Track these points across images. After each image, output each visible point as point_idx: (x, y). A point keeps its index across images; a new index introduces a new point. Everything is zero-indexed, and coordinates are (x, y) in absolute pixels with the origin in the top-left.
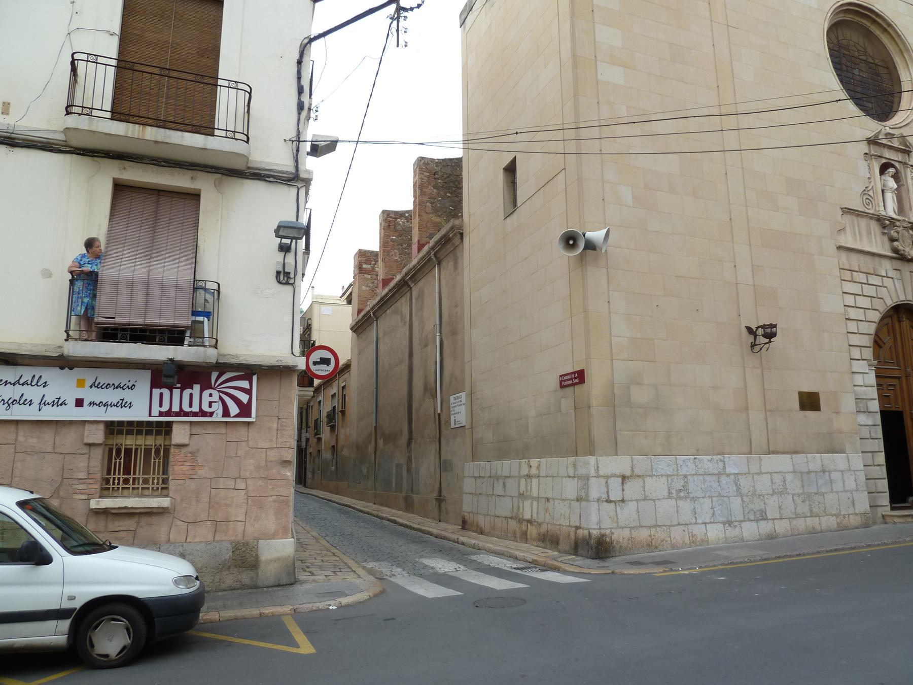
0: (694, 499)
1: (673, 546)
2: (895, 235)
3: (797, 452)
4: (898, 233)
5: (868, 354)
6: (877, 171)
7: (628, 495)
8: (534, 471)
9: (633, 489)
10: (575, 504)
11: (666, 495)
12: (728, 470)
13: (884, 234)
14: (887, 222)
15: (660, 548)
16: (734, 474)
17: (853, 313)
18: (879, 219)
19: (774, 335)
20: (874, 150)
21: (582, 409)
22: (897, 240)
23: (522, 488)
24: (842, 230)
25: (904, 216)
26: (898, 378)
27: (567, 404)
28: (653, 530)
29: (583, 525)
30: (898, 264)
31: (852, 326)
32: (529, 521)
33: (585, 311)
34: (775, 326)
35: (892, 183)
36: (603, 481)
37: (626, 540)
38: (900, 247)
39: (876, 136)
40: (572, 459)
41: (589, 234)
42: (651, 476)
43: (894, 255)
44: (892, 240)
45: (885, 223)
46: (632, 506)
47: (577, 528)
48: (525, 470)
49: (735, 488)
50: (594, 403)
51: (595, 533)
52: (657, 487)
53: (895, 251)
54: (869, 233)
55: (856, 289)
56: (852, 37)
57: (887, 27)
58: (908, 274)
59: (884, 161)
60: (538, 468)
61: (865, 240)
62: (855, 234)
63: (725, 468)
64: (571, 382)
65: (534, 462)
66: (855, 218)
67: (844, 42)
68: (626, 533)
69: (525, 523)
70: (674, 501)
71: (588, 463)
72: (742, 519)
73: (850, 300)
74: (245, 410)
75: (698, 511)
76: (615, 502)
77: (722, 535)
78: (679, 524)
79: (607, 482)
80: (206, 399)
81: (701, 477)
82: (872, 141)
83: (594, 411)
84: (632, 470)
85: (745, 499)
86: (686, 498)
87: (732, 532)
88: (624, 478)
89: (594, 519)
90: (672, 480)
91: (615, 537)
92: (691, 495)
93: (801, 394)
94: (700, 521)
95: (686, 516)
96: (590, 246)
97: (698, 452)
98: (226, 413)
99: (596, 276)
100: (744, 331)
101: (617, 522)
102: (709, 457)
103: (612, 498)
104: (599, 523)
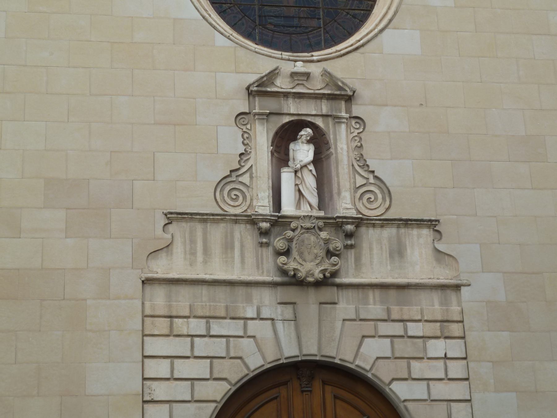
18: (252, 221)
30: (292, 293)
45: (272, 227)
53: (284, 272)
54: (228, 246)
55: (180, 347)
59: (286, 119)
62: (193, 253)
73: (160, 369)
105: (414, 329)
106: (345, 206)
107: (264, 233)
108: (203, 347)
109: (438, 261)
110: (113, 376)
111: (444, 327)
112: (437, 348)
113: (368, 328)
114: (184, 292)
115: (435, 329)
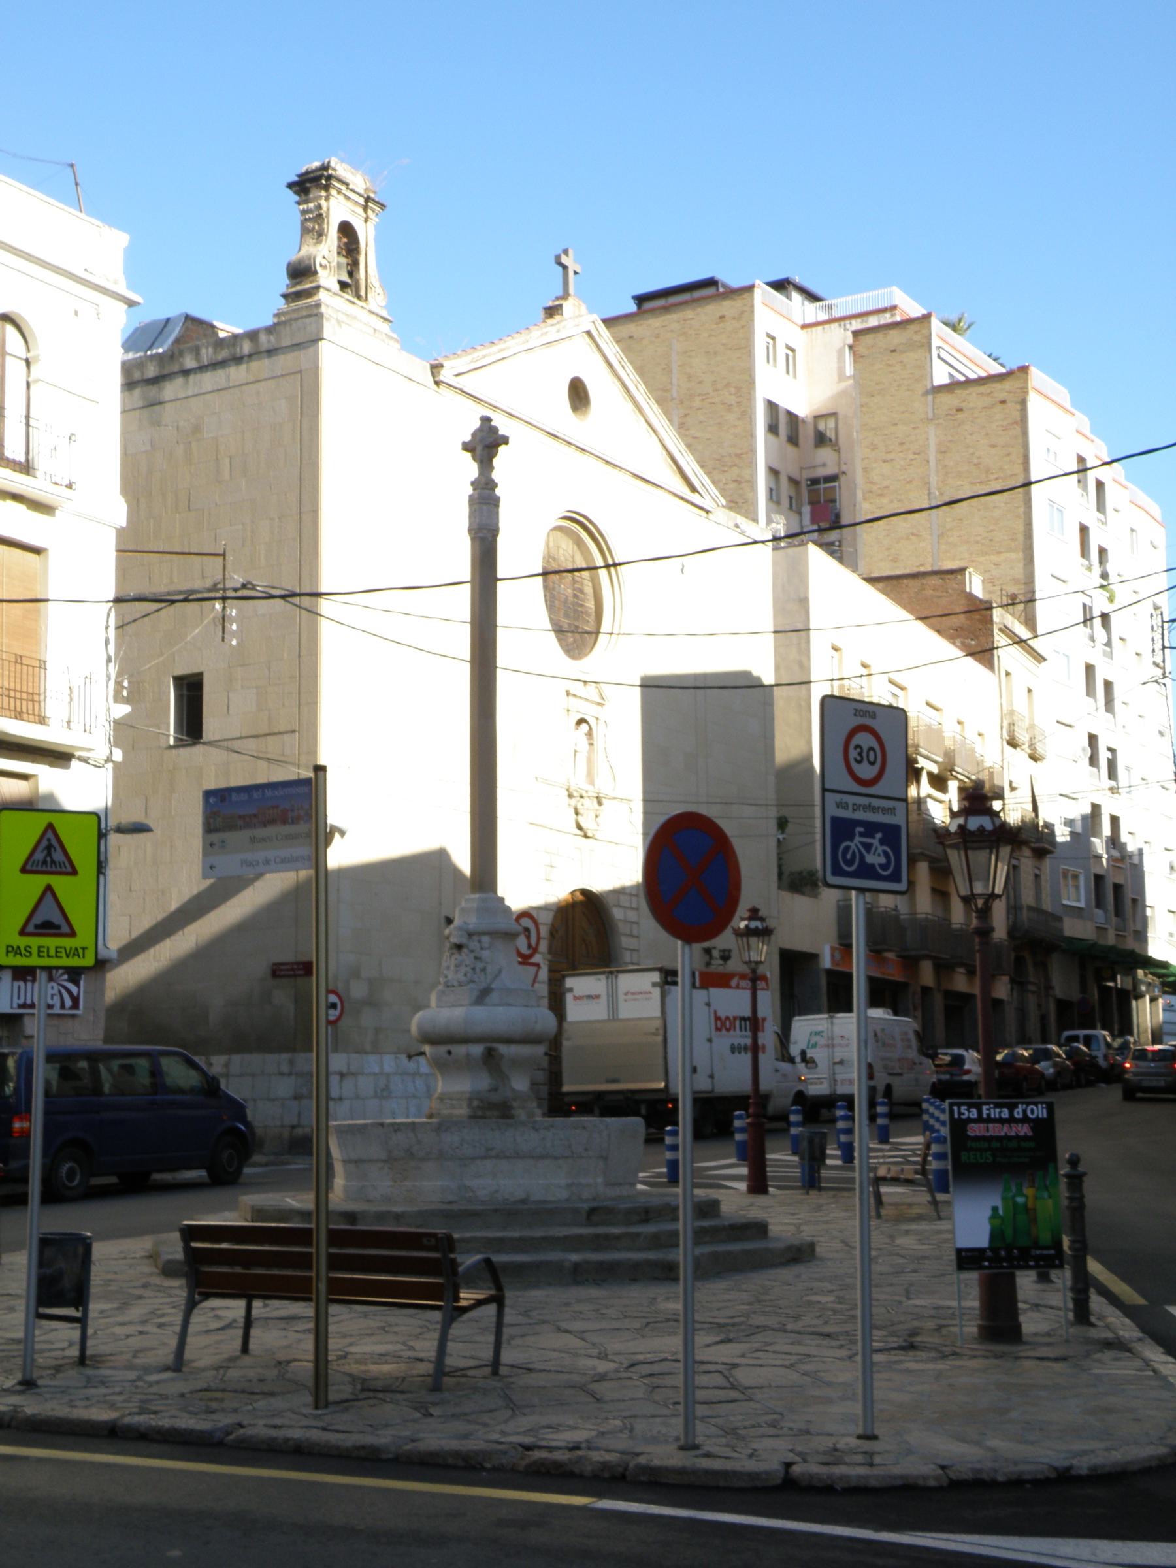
9: (348, 1084)
21: (303, 1002)
40: (285, 1056)
46: (347, 1103)
47: (293, 1127)
60: (227, 1065)
74: (75, 1001)
80: (50, 992)
98: (63, 1006)
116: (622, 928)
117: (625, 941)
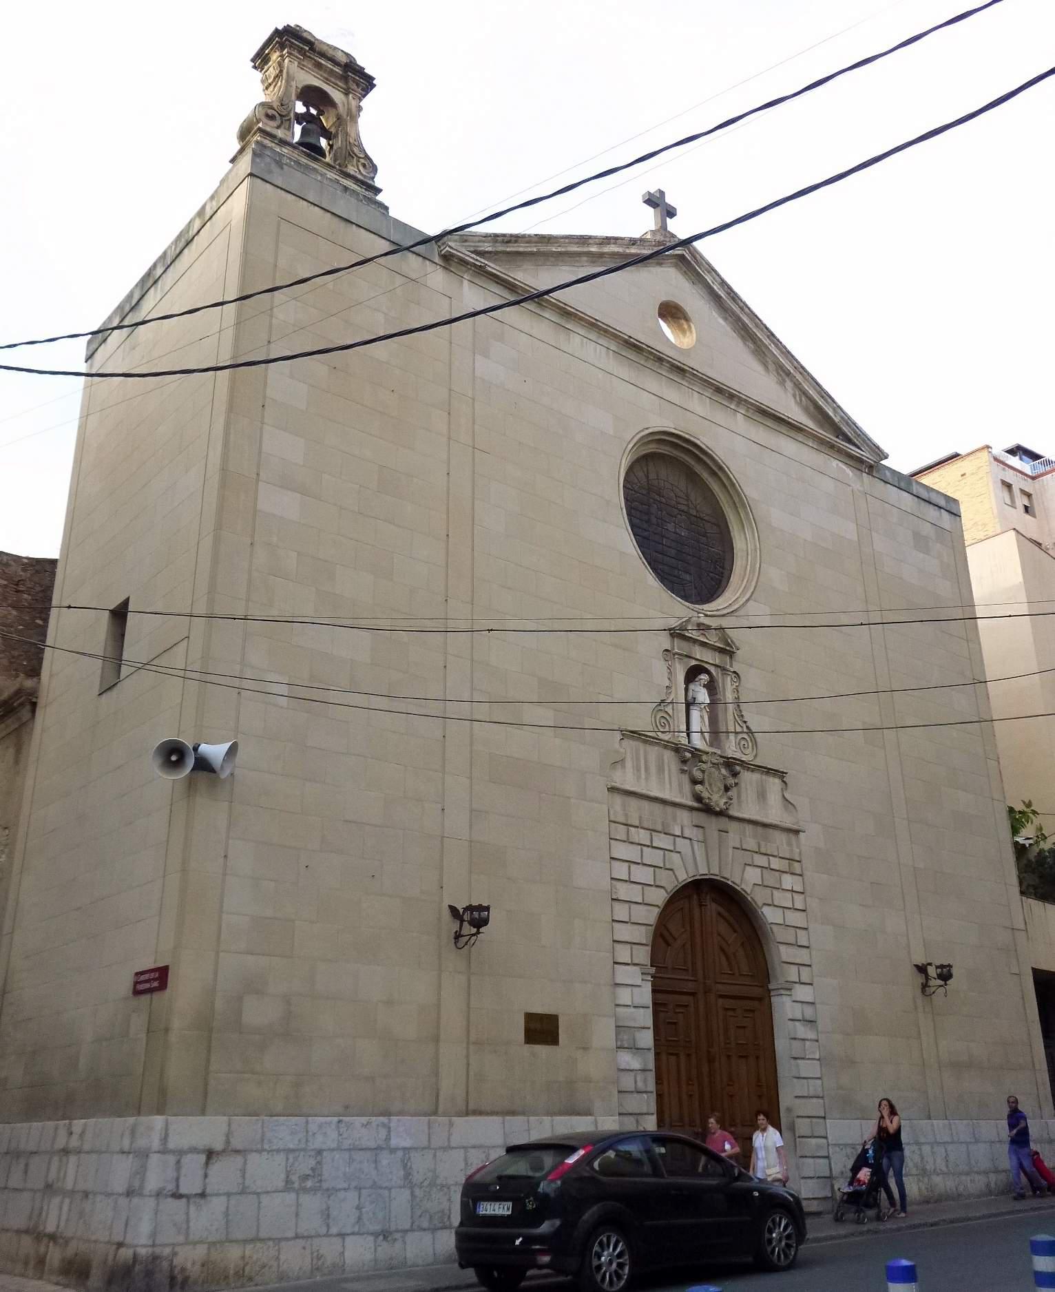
0: (330, 1192)
1: (282, 1277)
2: (698, 775)
3: (513, 1113)
4: (703, 772)
5: (643, 955)
6: (681, 677)
7: (214, 1184)
8: (74, 1142)
9: (224, 1174)
10: (123, 1201)
11: (281, 1184)
12: (394, 1142)
13: (683, 771)
14: (688, 755)
15: (258, 1279)
16: (404, 1149)
17: (623, 891)
18: (677, 749)
19: (485, 922)
20: (679, 646)
21: (156, 1030)
22: (701, 783)
23: (53, 1175)
24: (619, 763)
25: (719, 747)
26: (693, 994)
27: (138, 1024)
28: (249, 1247)
29: (128, 1240)
30: (701, 818)
31: (621, 912)
32: (53, 1237)
33: (184, 871)
34: (487, 909)
35: (703, 696)
36: (172, 1159)
37: (197, 1268)
38: (705, 795)
39: (683, 628)
40: (131, 1120)
41: (204, 748)
42: (260, 1151)
43: (696, 805)
44: (695, 782)
45: (687, 757)
46: (217, 1205)
47: (120, 1245)
48: (61, 1142)
49: (402, 1173)
50: (176, 1024)
51: (143, 1251)
52: (266, 1170)
53: (698, 798)
54: (660, 769)
55: (630, 852)
56: (668, 478)
57: (717, 470)
58: (716, 834)
59: (694, 663)
60: (82, 1135)
61: (654, 778)
62: (639, 770)
63: (388, 1139)
64: (147, 986)
65: (78, 1125)
66: (641, 746)
67: (655, 483)
68: (200, 1252)
69: (45, 1240)
70: (293, 1195)
71: (150, 1128)
72: (407, 1226)
73: (621, 871)
75: (334, 1213)
76: (187, 1197)
77: (369, 1256)
78: (297, 1237)
79: (178, 1162)
81: (346, 1155)
82: (677, 634)
83: (173, 1038)
84: (228, 1142)
85: (417, 1192)
86: (314, 1190)
87: (386, 1250)
88: (210, 1154)
89: (145, 1228)
90: (296, 1159)
91: (178, 1261)
92: (325, 1185)
93: (530, 1017)
94: (334, 1230)
95: (311, 1223)
96: (203, 765)
97: (347, 1110)
99: (211, 812)
100: (446, 913)
101: (187, 1235)
102: (364, 1120)
103: (183, 1190)
104: (153, 1235)
105: (776, 864)
106: (731, 748)
107: (684, 762)
108: (652, 857)
109: (786, 808)
110: (592, 874)
111: (793, 864)
112: (788, 881)
113: (747, 857)
114: (633, 803)
115: (783, 865)
116: (780, 934)
117: (785, 953)
